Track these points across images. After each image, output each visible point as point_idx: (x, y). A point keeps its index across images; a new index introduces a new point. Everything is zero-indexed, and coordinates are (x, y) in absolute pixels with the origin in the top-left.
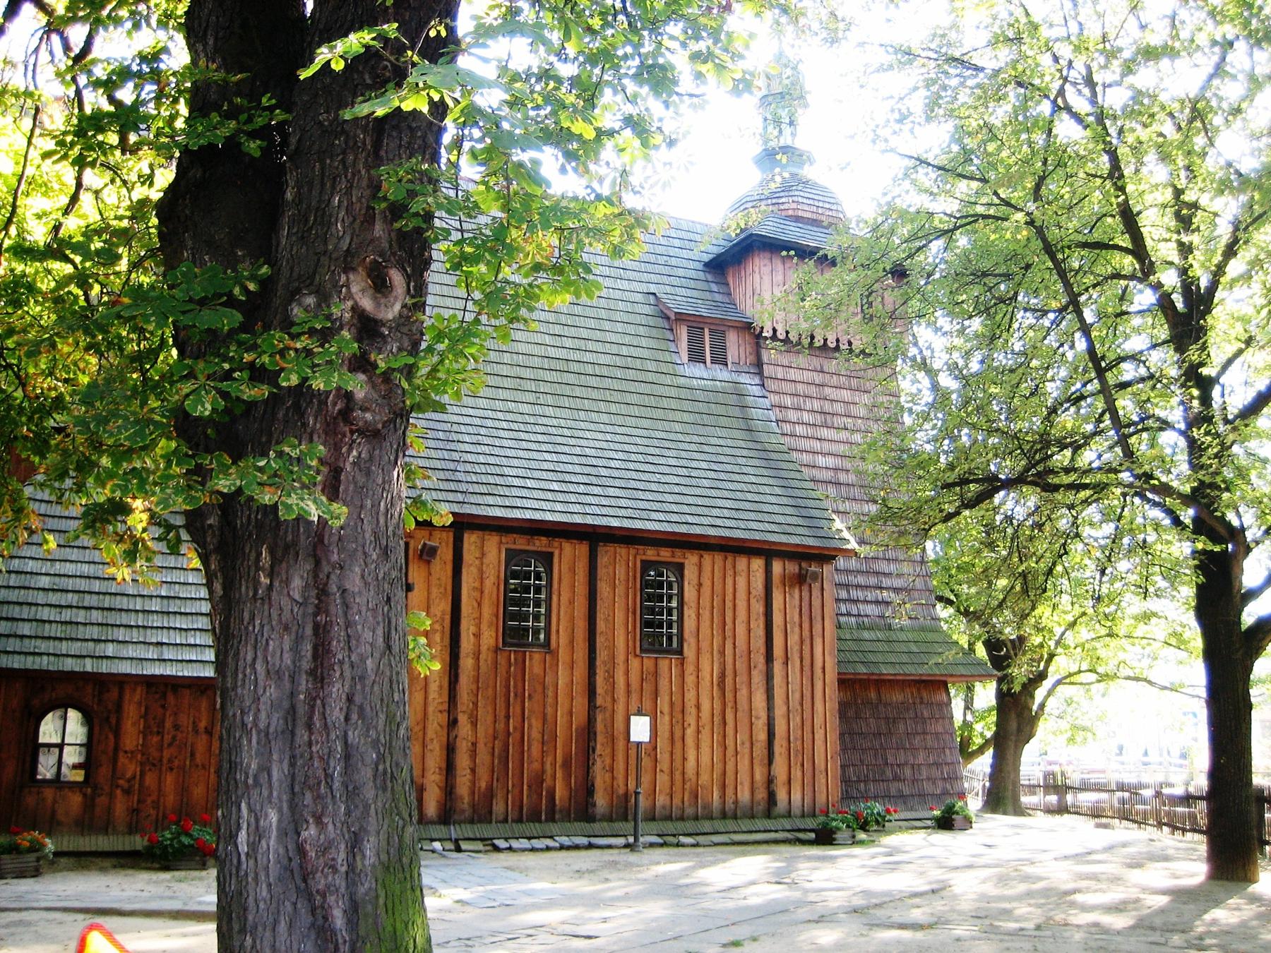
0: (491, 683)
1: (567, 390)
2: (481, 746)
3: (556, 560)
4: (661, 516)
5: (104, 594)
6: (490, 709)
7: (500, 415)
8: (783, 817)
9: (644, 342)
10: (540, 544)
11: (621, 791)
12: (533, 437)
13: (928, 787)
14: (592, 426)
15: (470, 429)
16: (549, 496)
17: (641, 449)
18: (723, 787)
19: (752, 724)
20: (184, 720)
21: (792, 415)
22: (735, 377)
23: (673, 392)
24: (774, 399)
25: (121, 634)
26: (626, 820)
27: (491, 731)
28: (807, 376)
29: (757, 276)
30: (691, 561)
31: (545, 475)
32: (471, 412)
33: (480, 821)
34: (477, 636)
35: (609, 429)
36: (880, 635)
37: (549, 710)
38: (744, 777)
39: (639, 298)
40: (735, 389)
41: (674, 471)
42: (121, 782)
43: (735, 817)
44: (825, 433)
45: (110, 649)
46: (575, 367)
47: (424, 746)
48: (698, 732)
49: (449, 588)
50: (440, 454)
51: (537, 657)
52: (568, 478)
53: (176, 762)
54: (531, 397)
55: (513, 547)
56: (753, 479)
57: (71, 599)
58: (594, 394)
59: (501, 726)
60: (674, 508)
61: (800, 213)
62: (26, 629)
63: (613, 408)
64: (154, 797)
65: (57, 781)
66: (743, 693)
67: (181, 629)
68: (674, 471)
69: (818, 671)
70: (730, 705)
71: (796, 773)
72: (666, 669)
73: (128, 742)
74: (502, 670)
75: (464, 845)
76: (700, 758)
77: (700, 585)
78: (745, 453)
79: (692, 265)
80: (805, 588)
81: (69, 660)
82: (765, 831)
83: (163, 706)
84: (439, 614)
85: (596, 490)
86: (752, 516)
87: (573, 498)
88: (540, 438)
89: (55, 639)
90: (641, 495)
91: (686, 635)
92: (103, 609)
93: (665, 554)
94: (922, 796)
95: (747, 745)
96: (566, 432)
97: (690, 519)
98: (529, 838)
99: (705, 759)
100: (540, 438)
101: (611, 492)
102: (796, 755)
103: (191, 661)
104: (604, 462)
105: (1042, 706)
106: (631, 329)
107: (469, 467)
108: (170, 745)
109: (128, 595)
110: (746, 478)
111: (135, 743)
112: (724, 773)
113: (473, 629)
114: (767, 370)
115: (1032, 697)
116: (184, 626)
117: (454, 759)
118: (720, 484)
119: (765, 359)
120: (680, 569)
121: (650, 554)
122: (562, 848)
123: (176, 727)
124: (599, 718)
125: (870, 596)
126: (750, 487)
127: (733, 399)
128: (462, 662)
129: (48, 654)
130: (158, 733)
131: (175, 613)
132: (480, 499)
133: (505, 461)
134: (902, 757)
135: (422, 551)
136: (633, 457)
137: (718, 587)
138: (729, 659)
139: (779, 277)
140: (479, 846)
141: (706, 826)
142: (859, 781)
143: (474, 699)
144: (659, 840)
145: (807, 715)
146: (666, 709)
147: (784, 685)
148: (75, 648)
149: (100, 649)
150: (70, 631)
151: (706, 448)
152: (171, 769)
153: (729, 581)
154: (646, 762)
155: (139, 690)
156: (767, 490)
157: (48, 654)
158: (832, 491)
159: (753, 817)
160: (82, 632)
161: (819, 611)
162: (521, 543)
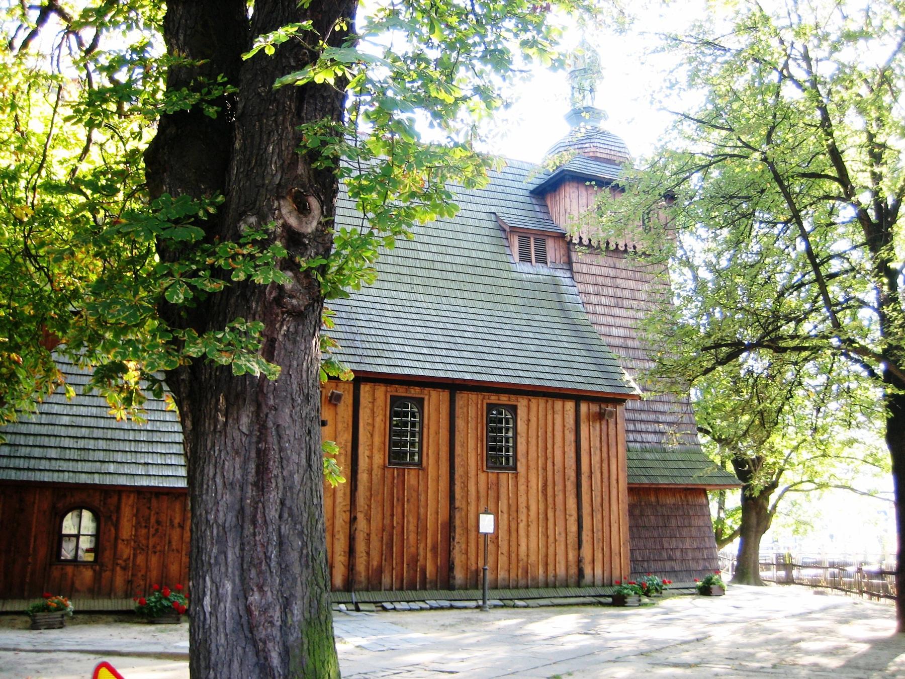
0: (381, 491)
1: (433, 282)
2: (374, 537)
3: (426, 403)
4: (501, 372)
6: (380, 509)
7: (386, 301)
8: (589, 586)
9: (487, 248)
10: (415, 392)
11: (473, 568)
12: (409, 316)
13: (693, 565)
14: (451, 308)
15: (364, 311)
16: (421, 358)
17: (486, 324)
18: (546, 564)
19: (566, 520)
20: (163, 518)
21: (594, 299)
22: (552, 272)
23: (508, 283)
24: (581, 287)
25: (119, 457)
26: (477, 588)
27: (380, 525)
28: (605, 271)
29: (568, 200)
30: (522, 403)
31: (418, 343)
32: (365, 298)
33: (373, 589)
34: (370, 457)
35: (463, 309)
36: (658, 456)
37: (422, 511)
38: (561, 558)
39: (483, 216)
41: (510, 339)
42: (120, 562)
43: (555, 587)
44: (617, 311)
45: (112, 468)
46: (438, 266)
47: (333, 536)
48: (528, 526)
50: (343, 328)
51: (413, 473)
52: (434, 345)
53: (158, 548)
54: (407, 288)
56: (566, 345)
57: (84, 432)
58: (453, 285)
59: (387, 521)
60: (510, 366)
61: (598, 155)
62: (53, 453)
63: (466, 295)
64: (143, 572)
65: (75, 561)
66: (560, 497)
67: (161, 453)
68: (510, 339)
69: (614, 482)
70: (550, 506)
71: (598, 555)
73: (124, 533)
74: (388, 481)
75: (361, 607)
76: (530, 545)
77: (529, 420)
78: (560, 326)
79: (521, 192)
80: (604, 423)
82: (576, 597)
83: (149, 508)
85: (454, 353)
86: (566, 371)
87: (438, 359)
88: (414, 317)
89: (73, 460)
90: (486, 356)
91: (520, 456)
92: (107, 439)
93: (504, 399)
94: (689, 571)
95: (563, 535)
96: (433, 312)
97: (521, 374)
98: (408, 602)
99: (533, 546)
100: (414, 317)
101: (465, 354)
102: (598, 542)
103: (168, 476)
104: (461, 334)
105: (775, 507)
106: (478, 238)
107: (364, 338)
108: (154, 535)
110: (561, 345)
112: (547, 556)
113: (367, 453)
114: (576, 267)
115: (767, 500)
118: (542, 349)
119: (574, 259)
120: (514, 409)
121: (493, 399)
122: (431, 608)
123: (158, 522)
124: (457, 515)
125: (650, 428)
126: (565, 351)
127: (551, 288)
129: (69, 471)
130: (146, 527)
131: (157, 442)
132: (371, 360)
133: (389, 333)
134: (674, 544)
135: (331, 397)
136: (480, 330)
137: (542, 422)
138: (550, 473)
139: (583, 201)
140: (372, 607)
141: (534, 593)
142: (643, 561)
143: (368, 503)
144: (501, 603)
145: (606, 513)
146: (505, 509)
148: (87, 467)
150: (84, 455)
151: (532, 323)
152: (155, 553)
153: (550, 417)
154: (491, 547)
155: (132, 496)
156: (576, 352)
157: (69, 471)
158: (622, 353)
159: (567, 586)
160: (92, 456)
161: (614, 440)
162: (401, 391)
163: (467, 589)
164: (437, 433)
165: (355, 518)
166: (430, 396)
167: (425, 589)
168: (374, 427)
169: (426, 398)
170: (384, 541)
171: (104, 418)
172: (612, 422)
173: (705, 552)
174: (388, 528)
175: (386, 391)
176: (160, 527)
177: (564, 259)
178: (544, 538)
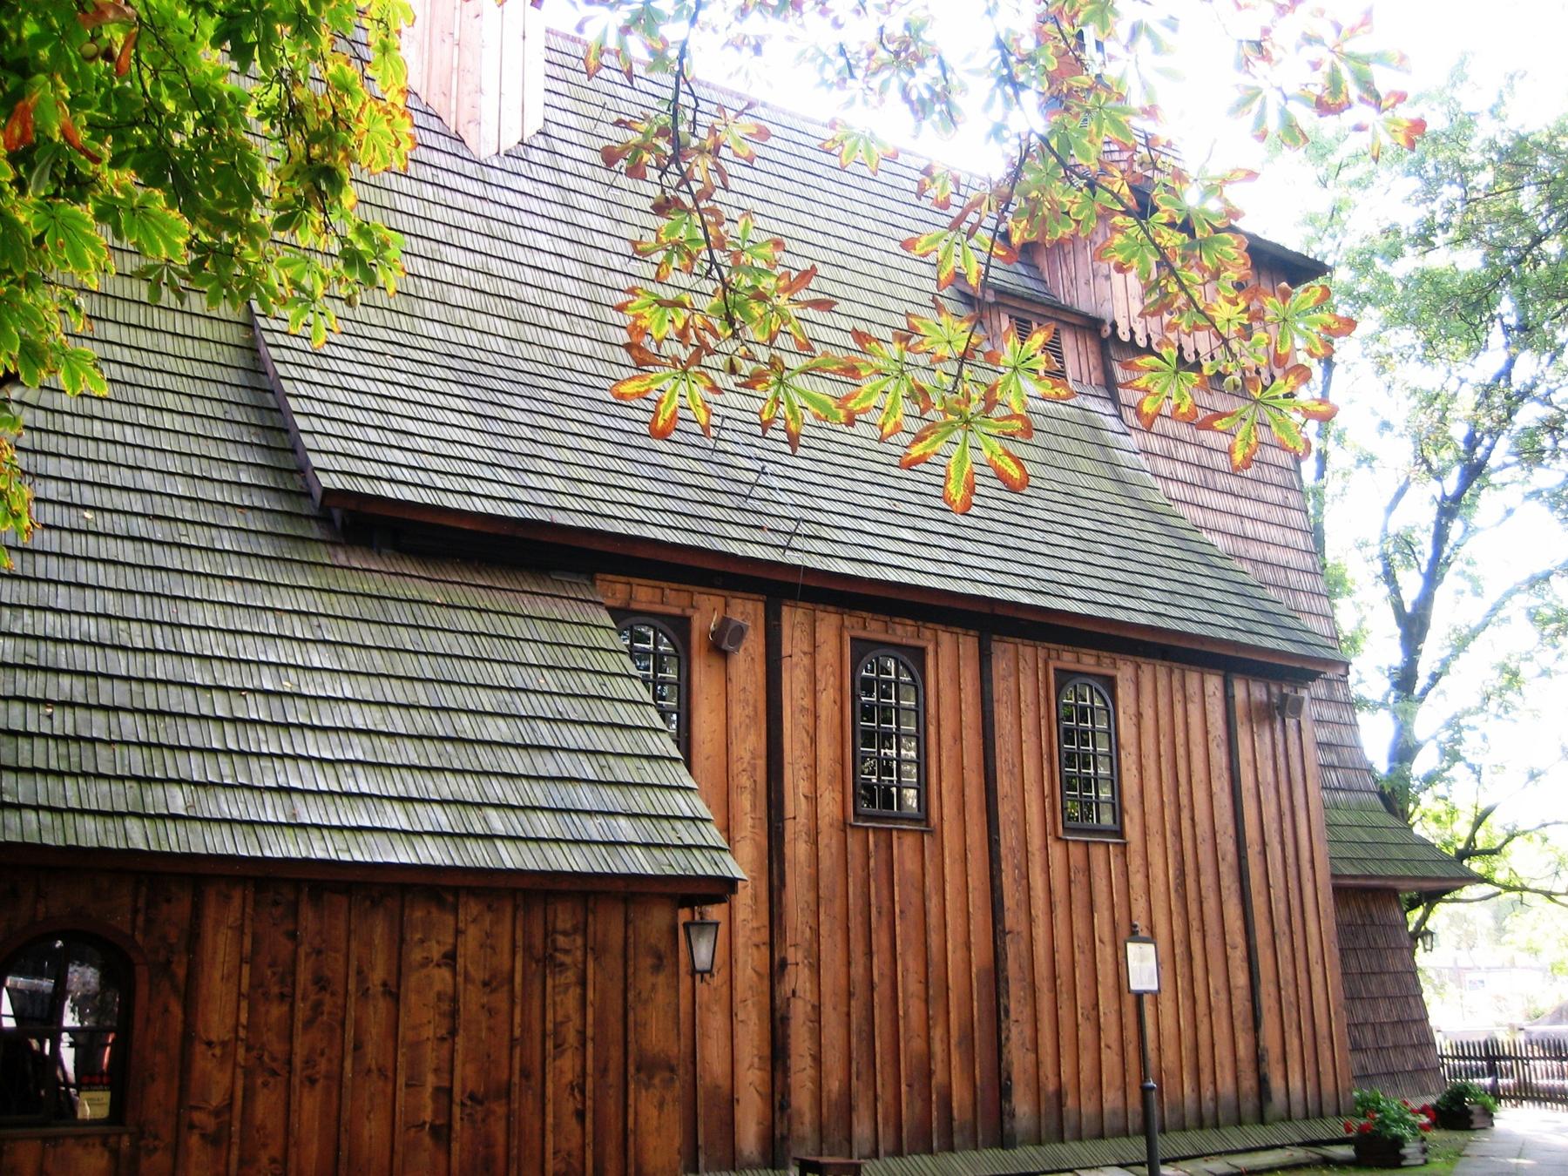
0: (839, 890)
5: (140, 681)
6: (839, 937)
8: (1283, 1120)
10: (903, 632)
13: (1395, 1060)
21: (1164, 467)
25: (194, 767)
30: (1124, 674)
34: (813, 799)
37: (934, 940)
40: (1086, 417)
42: (198, 1117)
45: (178, 800)
47: (732, 1015)
49: (762, 706)
51: (909, 842)
53: (323, 1066)
55: (863, 634)
57: (66, 687)
59: (858, 971)
64: (275, 1150)
67: (321, 760)
69: (1306, 866)
70: (1195, 924)
72: (1103, 865)
73: (215, 1018)
81: (89, 823)
83: (293, 936)
84: (747, 757)
89: (47, 772)
91: (1127, 804)
92: (145, 712)
95: (1223, 996)
99: (1168, 1022)
103: (360, 829)
108: (308, 1024)
109: (194, 686)
111: (230, 1022)
113: (804, 787)
116: (327, 755)
117: (786, 1036)
120: (1110, 683)
123: (321, 983)
127: (1084, 433)
128: (788, 850)
129: (37, 808)
130: (282, 996)
131: (301, 726)
138: (1188, 845)
147: (1264, 892)
148: (99, 795)
149: (155, 798)
150: (79, 757)
152: (312, 1081)
157: (37, 808)
162: (875, 629)
163: (1039, 1142)
164: (958, 738)
165: (784, 964)
166: (937, 644)
167: (951, 1148)
168: (816, 717)
169: (930, 649)
170: (854, 1027)
171: (124, 648)
172: (1291, 723)
173: (1414, 1029)
174: (860, 989)
175: (842, 627)
176: (327, 998)
177: (1097, 376)
178: (1188, 1004)
